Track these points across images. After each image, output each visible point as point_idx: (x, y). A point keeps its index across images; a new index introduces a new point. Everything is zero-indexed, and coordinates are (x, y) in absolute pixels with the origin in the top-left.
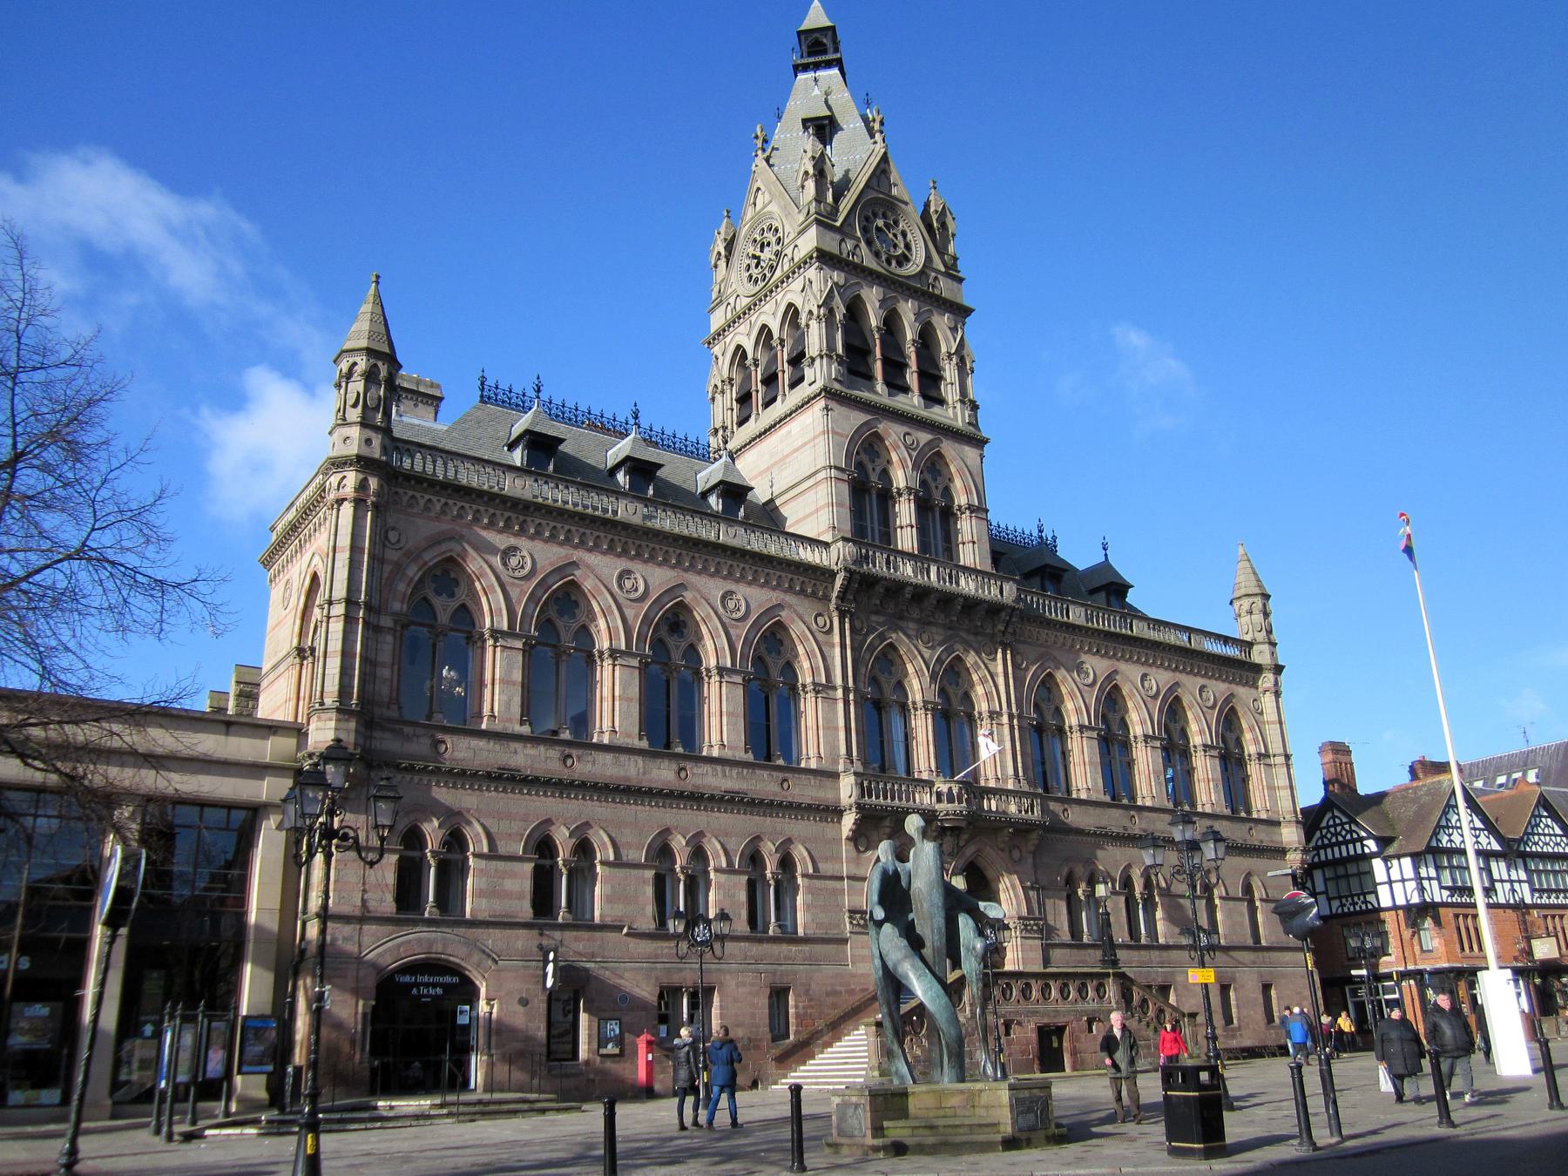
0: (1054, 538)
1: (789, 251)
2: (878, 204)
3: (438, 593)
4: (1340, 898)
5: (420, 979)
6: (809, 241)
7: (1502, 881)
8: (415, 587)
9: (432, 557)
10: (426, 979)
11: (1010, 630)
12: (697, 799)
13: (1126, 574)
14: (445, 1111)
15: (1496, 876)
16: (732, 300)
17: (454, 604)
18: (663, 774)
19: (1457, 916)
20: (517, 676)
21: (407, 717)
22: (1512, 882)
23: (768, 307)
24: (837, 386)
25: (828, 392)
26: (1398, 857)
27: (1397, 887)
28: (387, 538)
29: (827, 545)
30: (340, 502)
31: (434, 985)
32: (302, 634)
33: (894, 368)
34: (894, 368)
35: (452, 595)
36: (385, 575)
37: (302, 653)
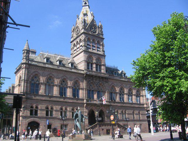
2: (93, 25)
6: (83, 31)
9: (34, 74)
18: (62, 100)
23: (78, 39)
25: (84, 51)
29: (84, 71)
30: (23, 68)
32: (19, 83)
37: (19, 85)
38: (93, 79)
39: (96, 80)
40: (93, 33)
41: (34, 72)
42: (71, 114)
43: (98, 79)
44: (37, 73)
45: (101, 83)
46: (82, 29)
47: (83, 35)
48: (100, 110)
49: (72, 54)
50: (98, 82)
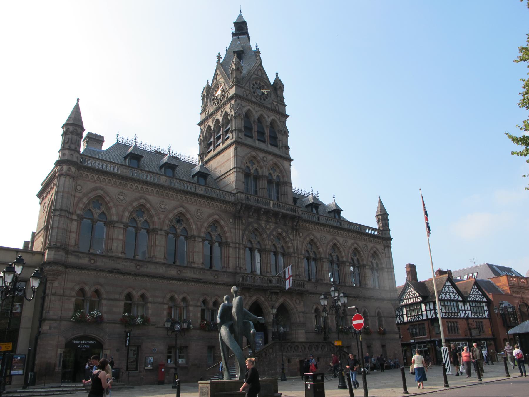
0: (318, 194)
1: (226, 95)
3: (94, 208)
4: (411, 316)
5: (81, 342)
6: (232, 91)
7: (462, 310)
8: (86, 206)
9: (92, 195)
10: (84, 342)
11: (298, 224)
12: (184, 280)
13: (341, 207)
14: (84, 388)
15: (460, 309)
16: (207, 111)
17: (100, 212)
18: (173, 272)
19: (447, 322)
20: (121, 237)
21: (81, 250)
22: (465, 310)
23: (219, 113)
24: (240, 140)
25: (235, 142)
26: (429, 302)
27: (429, 312)
28: (77, 188)
29: (234, 194)
31: (87, 344)
33: (261, 133)
34: (261, 133)
35: (99, 208)
36: (75, 201)
38: (259, 219)
39: (267, 221)
40: (260, 99)
41: (94, 189)
42: (199, 315)
43: (274, 220)
44: (102, 192)
45: (280, 230)
46: (230, 88)
47: (233, 102)
48: (277, 305)
49: (203, 153)
50: (272, 227)
